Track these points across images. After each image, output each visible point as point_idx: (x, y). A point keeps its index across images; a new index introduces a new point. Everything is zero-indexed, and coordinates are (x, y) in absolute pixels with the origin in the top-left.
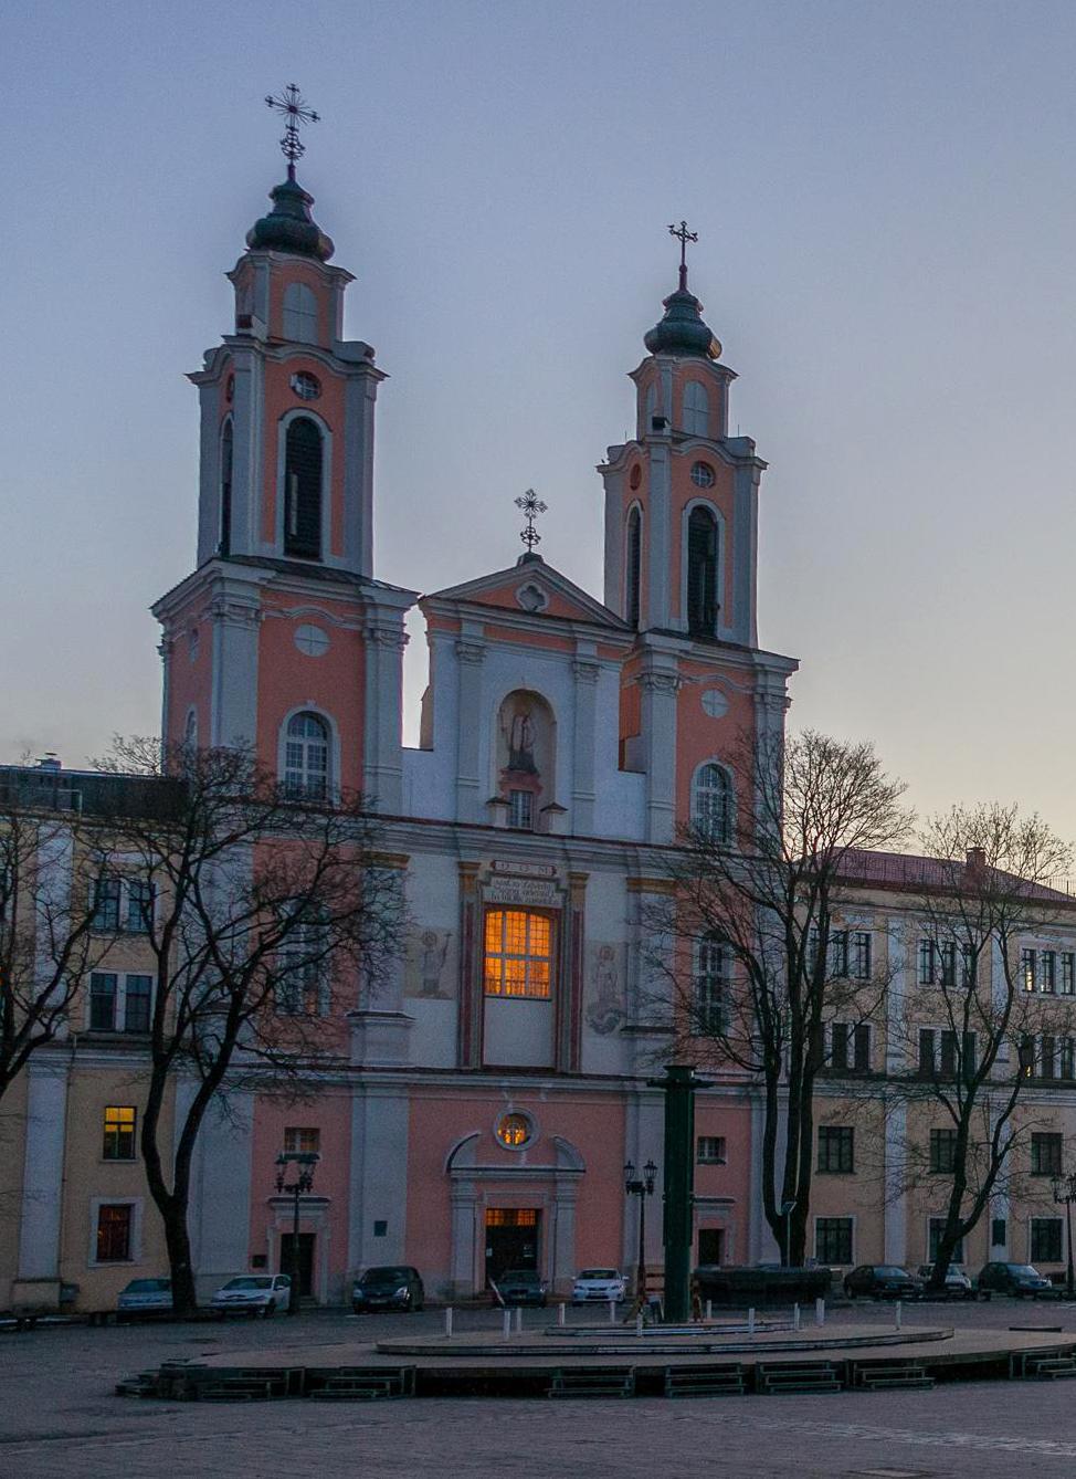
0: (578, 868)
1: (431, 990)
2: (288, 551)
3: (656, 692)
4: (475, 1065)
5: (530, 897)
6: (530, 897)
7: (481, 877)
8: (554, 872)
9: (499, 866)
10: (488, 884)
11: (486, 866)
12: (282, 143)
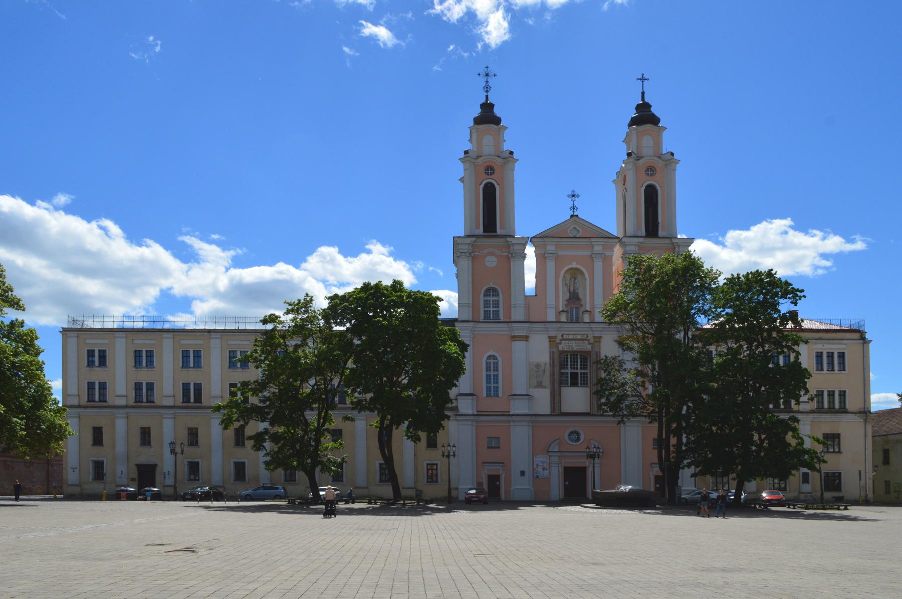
0: (597, 334)
1: (540, 385)
2: (484, 231)
4: (557, 412)
5: (578, 347)
6: (578, 347)
7: (558, 341)
8: (587, 336)
9: (565, 336)
10: (560, 343)
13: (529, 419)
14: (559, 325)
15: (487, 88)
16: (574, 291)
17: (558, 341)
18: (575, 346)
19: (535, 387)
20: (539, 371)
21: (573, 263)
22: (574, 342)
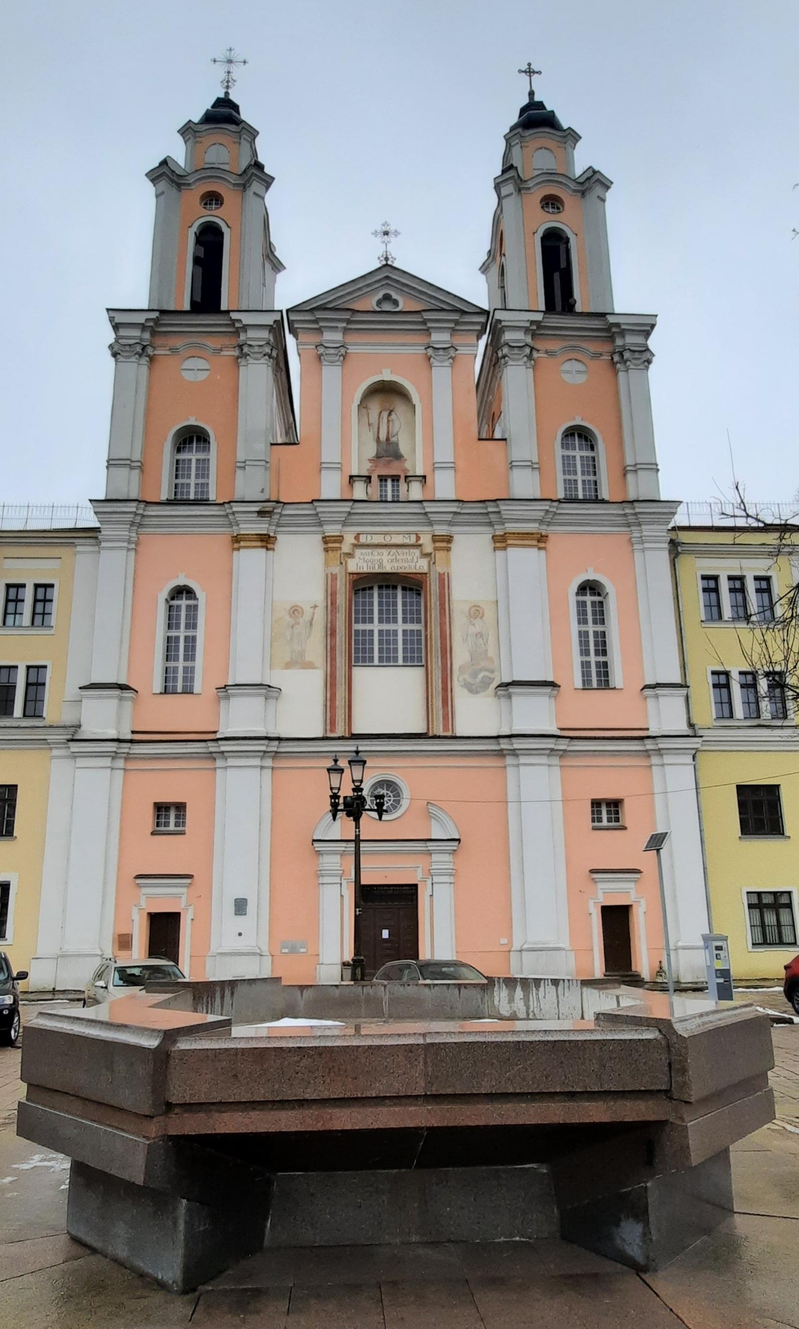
0: (441, 530)
1: (298, 662)
3: (511, 363)
4: (340, 731)
5: (396, 565)
6: (396, 565)
8: (418, 538)
10: (350, 555)
11: (349, 539)
12: (222, 82)
14: (346, 507)
15: (228, 82)
16: (388, 439)
17: (346, 548)
18: (388, 562)
19: (288, 666)
20: (298, 623)
21: (383, 371)
22: (385, 551)
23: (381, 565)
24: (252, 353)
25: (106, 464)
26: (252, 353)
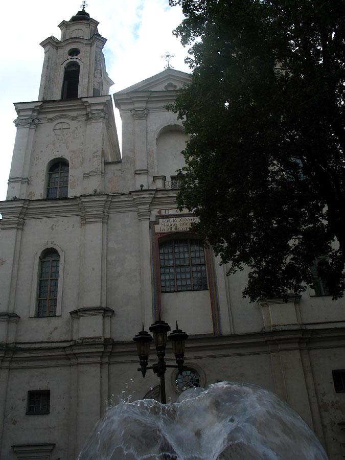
10: (157, 223)
13: (102, 350)
15: (84, 5)
23: (176, 228)
24: (95, 117)
25: (8, 182)
26: (95, 117)
